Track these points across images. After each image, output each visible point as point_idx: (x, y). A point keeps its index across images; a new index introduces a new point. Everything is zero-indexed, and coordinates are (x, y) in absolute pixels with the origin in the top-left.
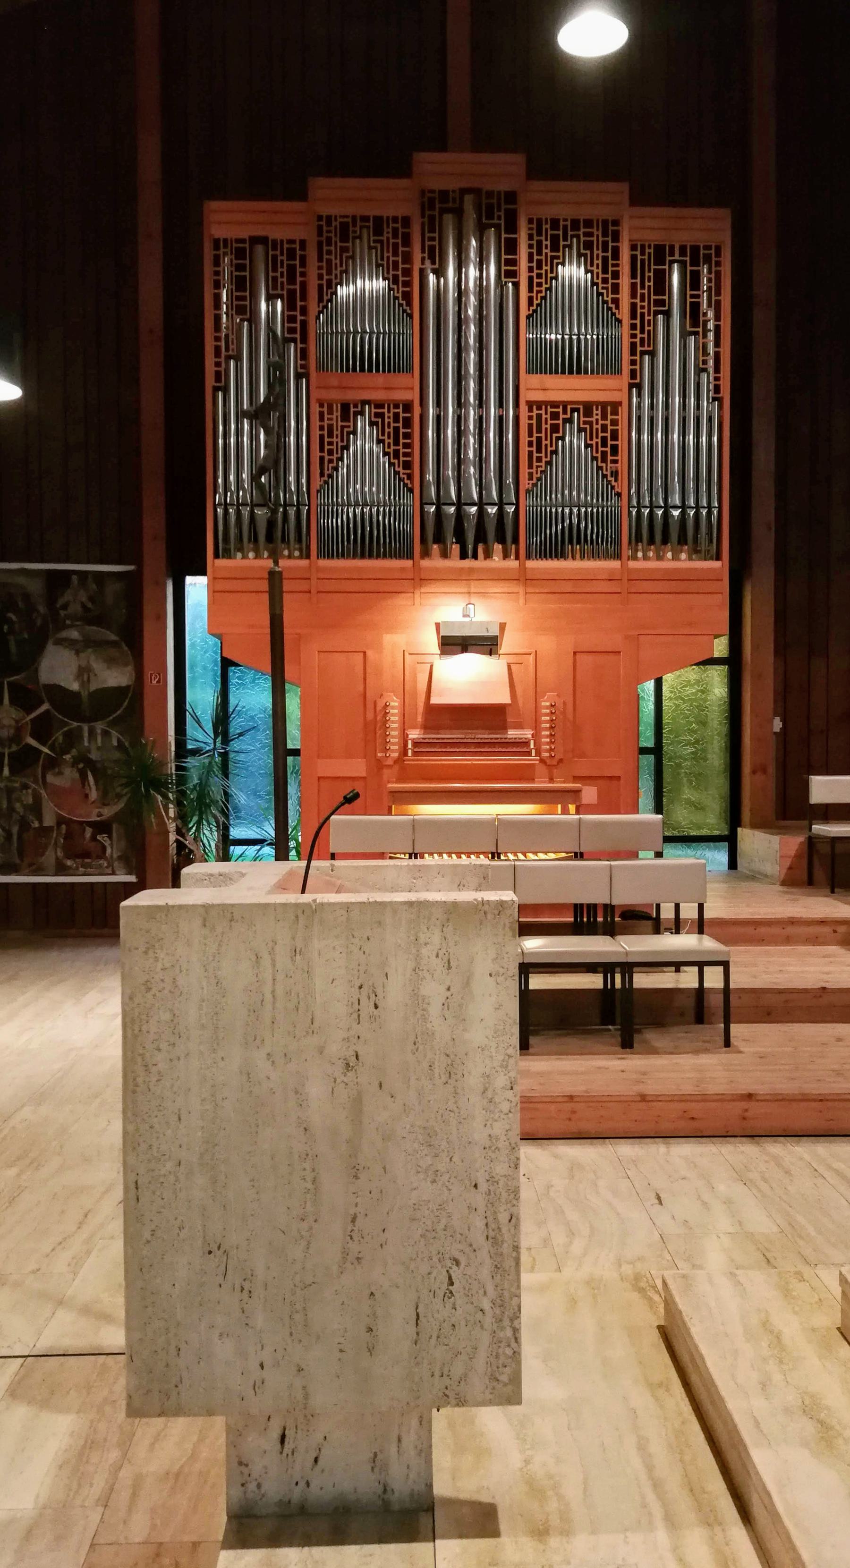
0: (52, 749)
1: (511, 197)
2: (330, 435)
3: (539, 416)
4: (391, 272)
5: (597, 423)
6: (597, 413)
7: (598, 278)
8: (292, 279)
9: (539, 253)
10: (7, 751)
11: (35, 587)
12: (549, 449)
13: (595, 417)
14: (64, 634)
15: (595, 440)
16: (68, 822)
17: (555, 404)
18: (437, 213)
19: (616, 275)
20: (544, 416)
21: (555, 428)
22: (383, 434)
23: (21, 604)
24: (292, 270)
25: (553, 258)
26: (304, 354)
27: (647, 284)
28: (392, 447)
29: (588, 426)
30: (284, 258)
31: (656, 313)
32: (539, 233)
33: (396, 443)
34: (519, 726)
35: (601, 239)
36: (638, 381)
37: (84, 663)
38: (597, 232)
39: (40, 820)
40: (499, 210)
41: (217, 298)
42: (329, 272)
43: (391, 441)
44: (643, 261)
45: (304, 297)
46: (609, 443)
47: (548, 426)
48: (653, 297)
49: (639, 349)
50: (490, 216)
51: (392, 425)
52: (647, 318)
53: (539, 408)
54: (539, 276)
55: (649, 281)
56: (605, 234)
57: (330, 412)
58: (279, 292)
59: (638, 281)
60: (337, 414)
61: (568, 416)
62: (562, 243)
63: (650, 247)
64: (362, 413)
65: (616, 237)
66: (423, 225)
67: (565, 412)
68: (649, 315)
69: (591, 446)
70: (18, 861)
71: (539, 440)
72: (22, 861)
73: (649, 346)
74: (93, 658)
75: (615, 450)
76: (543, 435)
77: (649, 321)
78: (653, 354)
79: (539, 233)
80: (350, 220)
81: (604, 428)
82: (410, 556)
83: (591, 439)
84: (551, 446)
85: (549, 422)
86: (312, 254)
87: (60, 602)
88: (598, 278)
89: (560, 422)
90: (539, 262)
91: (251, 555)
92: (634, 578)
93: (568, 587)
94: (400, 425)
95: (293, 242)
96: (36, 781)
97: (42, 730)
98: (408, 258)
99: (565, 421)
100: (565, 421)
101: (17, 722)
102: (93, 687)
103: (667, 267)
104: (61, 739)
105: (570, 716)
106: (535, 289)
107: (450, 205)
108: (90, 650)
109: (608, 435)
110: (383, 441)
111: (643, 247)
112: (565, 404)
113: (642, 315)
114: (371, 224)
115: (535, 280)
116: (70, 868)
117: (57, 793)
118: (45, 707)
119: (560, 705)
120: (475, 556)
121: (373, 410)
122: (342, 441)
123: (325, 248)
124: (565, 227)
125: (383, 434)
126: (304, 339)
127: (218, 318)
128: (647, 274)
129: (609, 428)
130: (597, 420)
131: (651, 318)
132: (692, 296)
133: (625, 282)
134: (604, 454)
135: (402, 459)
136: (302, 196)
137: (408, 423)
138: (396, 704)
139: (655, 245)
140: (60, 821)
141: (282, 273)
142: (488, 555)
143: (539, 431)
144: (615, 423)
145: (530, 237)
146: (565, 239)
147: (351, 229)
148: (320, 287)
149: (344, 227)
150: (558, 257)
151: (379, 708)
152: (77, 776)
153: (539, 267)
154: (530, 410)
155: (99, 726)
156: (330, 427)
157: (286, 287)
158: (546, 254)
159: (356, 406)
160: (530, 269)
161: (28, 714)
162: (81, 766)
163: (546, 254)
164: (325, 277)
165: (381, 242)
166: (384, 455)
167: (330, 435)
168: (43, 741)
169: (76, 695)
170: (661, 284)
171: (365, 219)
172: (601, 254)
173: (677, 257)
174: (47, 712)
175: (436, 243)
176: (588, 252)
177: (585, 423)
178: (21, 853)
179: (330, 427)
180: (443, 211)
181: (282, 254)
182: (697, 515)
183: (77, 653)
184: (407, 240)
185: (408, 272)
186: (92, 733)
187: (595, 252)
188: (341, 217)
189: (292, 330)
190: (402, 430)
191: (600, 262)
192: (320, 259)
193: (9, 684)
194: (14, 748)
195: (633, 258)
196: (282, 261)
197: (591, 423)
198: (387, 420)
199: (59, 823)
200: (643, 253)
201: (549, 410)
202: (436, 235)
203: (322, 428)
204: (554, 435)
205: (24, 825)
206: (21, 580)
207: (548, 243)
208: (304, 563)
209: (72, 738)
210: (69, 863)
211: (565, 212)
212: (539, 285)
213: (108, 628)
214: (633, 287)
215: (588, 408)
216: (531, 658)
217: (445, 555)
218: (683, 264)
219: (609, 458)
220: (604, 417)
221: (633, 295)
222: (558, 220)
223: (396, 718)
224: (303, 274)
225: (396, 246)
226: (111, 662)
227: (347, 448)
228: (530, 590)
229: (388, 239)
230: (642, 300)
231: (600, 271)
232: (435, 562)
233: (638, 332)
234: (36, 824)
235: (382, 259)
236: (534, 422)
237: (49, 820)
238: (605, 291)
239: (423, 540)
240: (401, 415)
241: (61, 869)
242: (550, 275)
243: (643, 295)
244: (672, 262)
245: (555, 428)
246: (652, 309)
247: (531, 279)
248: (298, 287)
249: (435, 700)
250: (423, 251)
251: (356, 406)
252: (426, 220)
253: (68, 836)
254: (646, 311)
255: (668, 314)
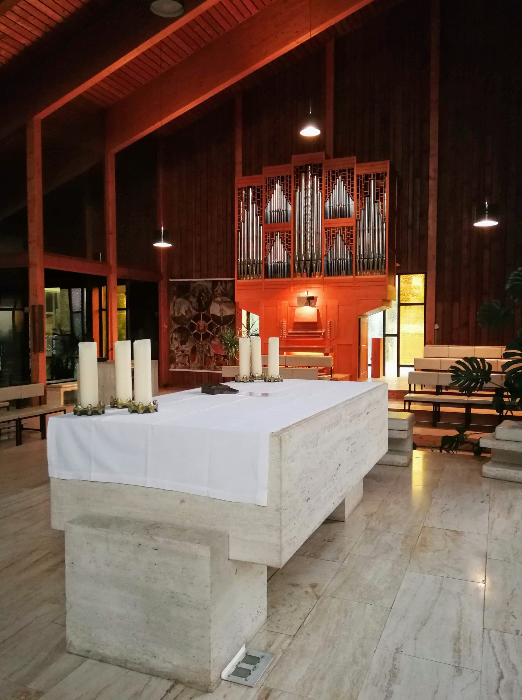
0: (213, 333)
1: (321, 165)
2: (268, 242)
3: (329, 232)
4: (286, 192)
5: (346, 233)
6: (346, 230)
7: (347, 187)
8: (258, 198)
9: (329, 182)
10: (201, 334)
11: (209, 286)
12: (332, 242)
13: (346, 231)
14: (216, 299)
15: (346, 238)
16: (217, 355)
17: (333, 228)
18: (299, 173)
19: (352, 186)
20: (330, 232)
21: (333, 236)
22: (283, 241)
23: (205, 291)
24: (258, 194)
25: (333, 183)
26: (261, 219)
27: (362, 187)
28: (286, 245)
29: (343, 234)
30: (257, 191)
31: (365, 197)
32: (329, 176)
33: (287, 243)
34: (321, 328)
35: (348, 175)
36: (359, 219)
37: (221, 308)
38: (347, 173)
39: (210, 354)
40: (317, 170)
41: (239, 205)
42: (269, 194)
43: (285, 243)
44: (361, 180)
45: (262, 203)
46: (350, 239)
47: (331, 235)
48: (364, 192)
49: (360, 208)
50: (314, 172)
51: (286, 238)
52: (362, 198)
53: (329, 229)
54: (329, 189)
55: (363, 187)
56: (349, 173)
57: (268, 235)
58: (255, 201)
59: (360, 187)
60: (270, 236)
61: (337, 231)
62: (336, 178)
63: (363, 176)
64: (277, 235)
65: (353, 174)
66: (295, 177)
67: (336, 230)
68: (363, 197)
69: (344, 240)
70: (204, 366)
71: (328, 239)
72: (205, 365)
73: (363, 207)
74: (224, 306)
75: (352, 241)
76: (330, 238)
77: (363, 199)
78: (364, 210)
79: (329, 176)
80: (274, 178)
81: (349, 234)
82: (290, 277)
83: (344, 238)
84: (332, 241)
85: (332, 234)
86: (264, 189)
87: (216, 290)
88: (347, 187)
89: (335, 233)
90: (329, 185)
91: (248, 278)
92: (355, 281)
93: (333, 285)
94: (288, 238)
95: (259, 186)
96: (209, 343)
97: (210, 327)
98: (290, 188)
99: (337, 233)
100: (337, 233)
101: (204, 325)
102: (224, 315)
103: (369, 182)
104: (215, 330)
105: (337, 325)
106: (328, 193)
107: (303, 170)
108: (223, 304)
109: (350, 236)
110: (283, 243)
111: (361, 176)
112: (336, 228)
113: (361, 197)
114: (280, 179)
115: (328, 190)
116: (217, 368)
117: (214, 346)
118: (212, 321)
119: (333, 321)
120: (310, 276)
121: (280, 234)
122: (272, 243)
123: (268, 187)
124: (337, 172)
125: (283, 241)
126: (262, 215)
127: (239, 211)
128: (362, 184)
129: (350, 234)
130: (346, 232)
131: (364, 198)
132: (377, 190)
133: (355, 188)
134: (348, 242)
135: (288, 248)
136: (261, 173)
137: (290, 237)
138: (285, 322)
139: (365, 175)
140: (215, 354)
141: (256, 196)
142: (315, 276)
143: (329, 236)
144: (352, 232)
145: (326, 177)
146: (337, 176)
147: (275, 181)
148: (266, 199)
149: (273, 180)
150: (335, 182)
151: (280, 323)
152: (219, 341)
153: (329, 186)
154: (326, 230)
155: (226, 326)
156: (268, 240)
157: (257, 200)
158: (331, 182)
159: (276, 233)
160: (326, 187)
161: (207, 323)
162: (221, 338)
163: (331, 182)
164: (268, 196)
165: (283, 184)
166: (283, 247)
167: (268, 242)
168: (211, 331)
169: (219, 317)
170: (367, 187)
171: (279, 177)
172: (348, 180)
173: (372, 177)
174: (212, 322)
175: (299, 182)
176: (344, 180)
177: (343, 233)
178: (205, 364)
179: (268, 240)
180: (301, 172)
181: (256, 190)
182: (378, 260)
183: (220, 304)
184: (290, 183)
185: (290, 192)
186: (223, 328)
187: (346, 179)
188: (272, 177)
189: (259, 212)
190: (288, 239)
191: (348, 182)
192: (266, 191)
193: (202, 314)
194: (203, 333)
195: (358, 180)
196: (256, 192)
197: (344, 233)
198: (284, 236)
199: (215, 356)
200: (361, 178)
201: (332, 230)
202: (299, 180)
203: (266, 240)
204: (333, 238)
205: (206, 355)
206: (205, 284)
207: (332, 178)
208: (261, 280)
209: (218, 330)
210: (217, 367)
211: (337, 169)
212: (329, 191)
213: (227, 297)
214: (358, 189)
215: (343, 228)
216: (325, 307)
217: (302, 276)
218: (374, 180)
219: (350, 244)
220: (349, 231)
221: (358, 191)
222: (335, 170)
223: (285, 326)
224: (262, 196)
225: (287, 184)
226: (228, 307)
227: (273, 245)
228: (325, 286)
229: (285, 183)
230: (361, 193)
231: (347, 185)
232: (299, 278)
233: (359, 203)
234: (209, 355)
235: (283, 189)
236: (327, 234)
237: (212, 354)
238: (349, 191)
239: (294, 271)
240: (288, 235)
241: (215, 369)
242: (332, 188)
243: (361, 191)
244: (371, 180)
245: (333, 236)
246: (364, 195)
247: (326, 190)
248: (260, 200)
249: (295, 321)
250: (295, 185)
251: (276, 233)
252: (296, 176)
253: (217, 359)
254: (362, 196)
255: (369, 196)
